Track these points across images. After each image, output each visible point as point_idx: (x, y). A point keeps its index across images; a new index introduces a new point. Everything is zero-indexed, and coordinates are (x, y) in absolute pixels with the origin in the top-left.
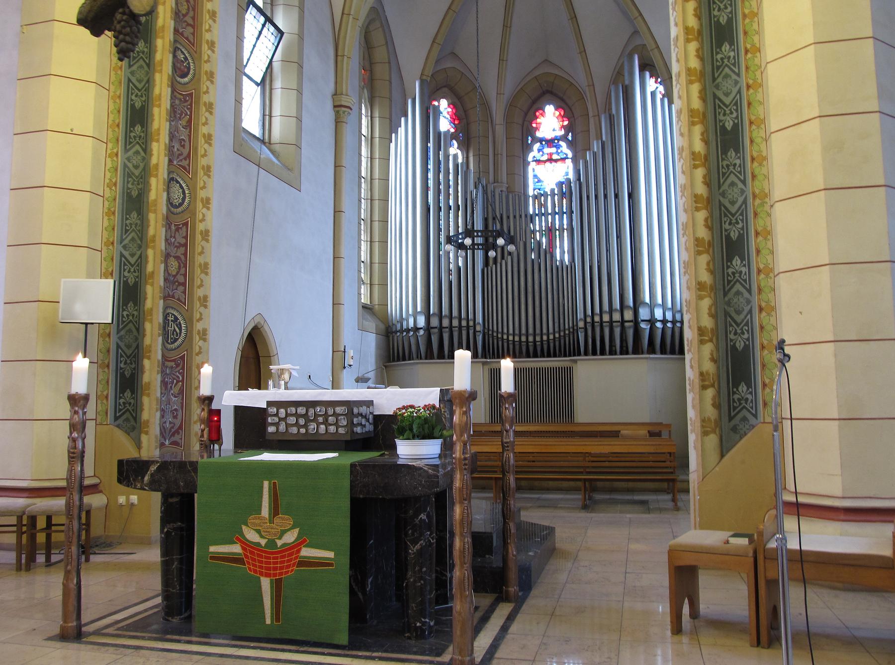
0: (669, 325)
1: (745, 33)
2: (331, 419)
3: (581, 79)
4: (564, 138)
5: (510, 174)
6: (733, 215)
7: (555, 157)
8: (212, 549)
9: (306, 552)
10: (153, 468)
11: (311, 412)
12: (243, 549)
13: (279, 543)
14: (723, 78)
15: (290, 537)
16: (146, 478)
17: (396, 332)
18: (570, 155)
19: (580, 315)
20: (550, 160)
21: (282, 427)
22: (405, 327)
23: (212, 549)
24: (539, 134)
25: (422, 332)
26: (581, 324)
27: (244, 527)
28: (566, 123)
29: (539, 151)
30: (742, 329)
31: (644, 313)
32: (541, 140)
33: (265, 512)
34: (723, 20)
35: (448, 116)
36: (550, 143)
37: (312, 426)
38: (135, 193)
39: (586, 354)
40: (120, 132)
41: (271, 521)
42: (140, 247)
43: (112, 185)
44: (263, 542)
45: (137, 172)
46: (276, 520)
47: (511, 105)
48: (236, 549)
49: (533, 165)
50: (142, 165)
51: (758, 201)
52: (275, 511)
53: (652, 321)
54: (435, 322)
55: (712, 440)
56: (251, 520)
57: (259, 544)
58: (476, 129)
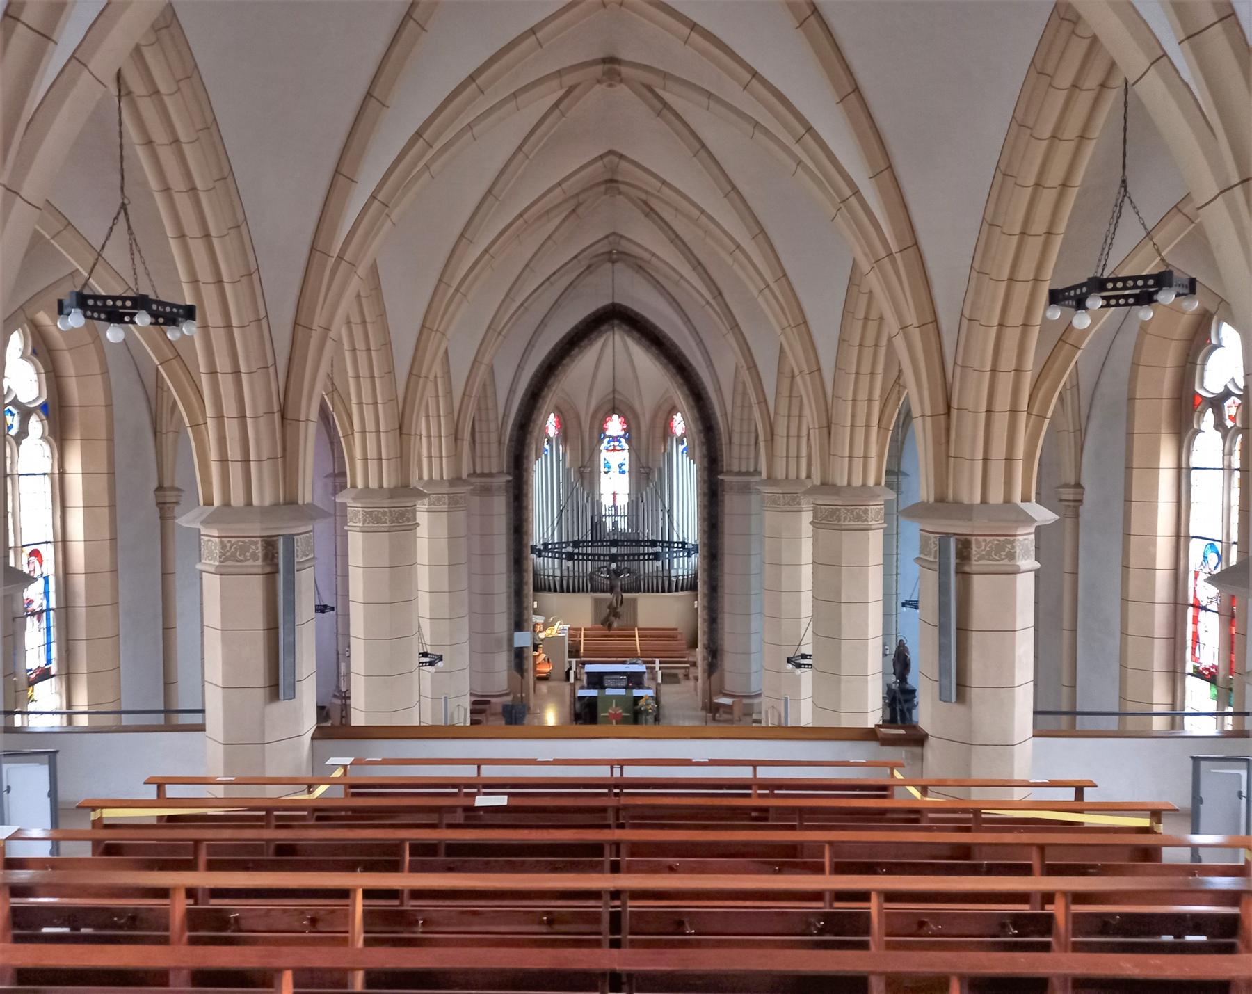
0: (686, 577)
3: (637, 406)
4: (623, 436)
5: (591, 455)
7: (618, 448)
9: (624, 714)
15: (620, 711)
17: (540, 575)
18: (627, 447)
19: (642, 572)
20: (614, 450)
22: (546, 573)
24: (608, 433)
25: (558, 579)
26: (642, 577)
28: (625, 427)
29: (609, 442)
31: (673, 573)
32: (610, 437)
33: (614, 706)
35: (554, 424)
36: (615, 439)
39: (644, 592)
43: (509, 587)
47: (594, 416)
49: (604, 454)
52: (616, 706)
53: (677, 577)
54: (565, 574)
55: (706, 675)
58: (572, 433)
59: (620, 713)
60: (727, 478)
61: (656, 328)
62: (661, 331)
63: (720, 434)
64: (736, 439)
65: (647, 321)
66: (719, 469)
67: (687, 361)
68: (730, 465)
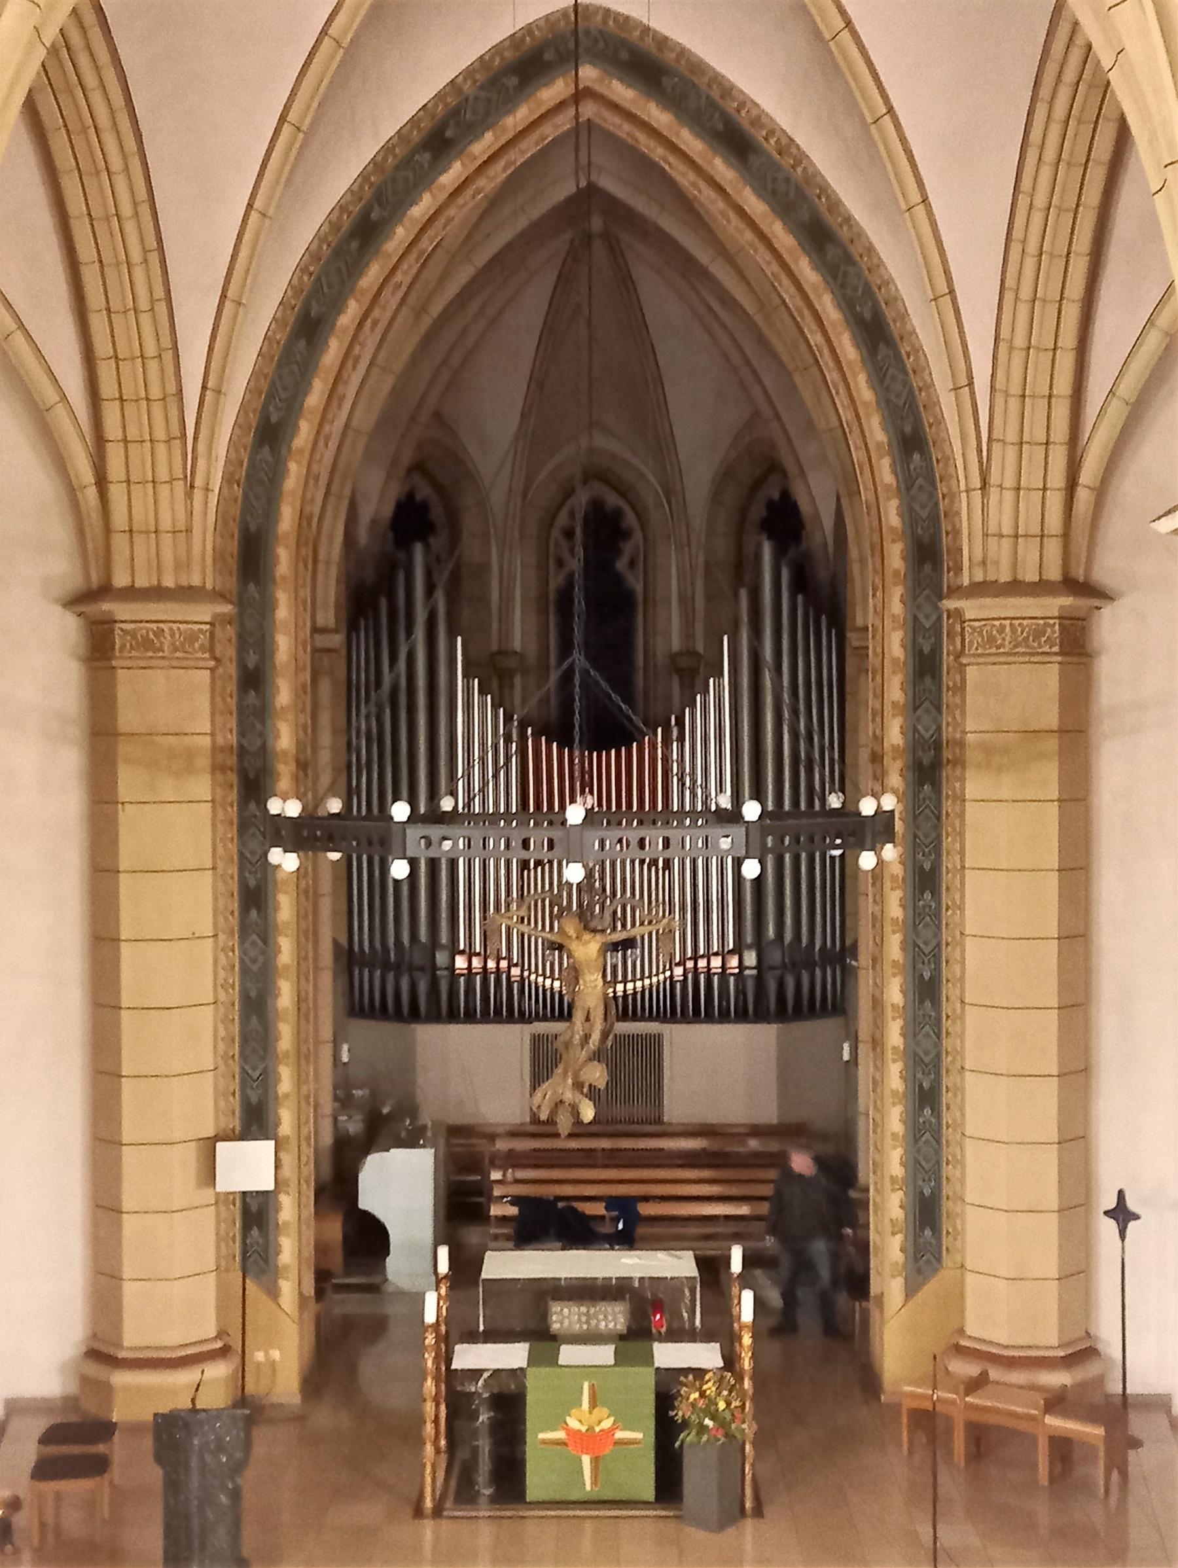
1: (948, 889)
2: (610, 1318)
6: (926, 1066)
8: (541, 1436)
9: (620, 1435)
10: (486, 1375)
11: (592, 1311)
12: (568, 1434)
13: (597, 1429)
14: (924, 926)
16: (481, 1383)
21: (566, 1323)
23: (541, 1436)
27: (568, 1419)
30: (930, 1177)
34: (927, 866)
37: (593, 1322)
38: (253, 994)
40: (234, 921)
41: (590, 1413)
42: (263, 1059)
44: (584, 1429)
45: (255, 968)
46: (596, 1411)
48: (560, 1435)
50: (261, 959)
51: (950, 1058)
52: (593, 1404)
56: (573, 1411)
57: (579, 1431)
59: (611, 1431)
60: (971, 608)
61: (728, 90)
62: (745, 102)
63: (948, 459)
64: (1003, 471)
65: (699, 67)
66: (947, 578)
67: (835, 205)
68: (984, 563)
